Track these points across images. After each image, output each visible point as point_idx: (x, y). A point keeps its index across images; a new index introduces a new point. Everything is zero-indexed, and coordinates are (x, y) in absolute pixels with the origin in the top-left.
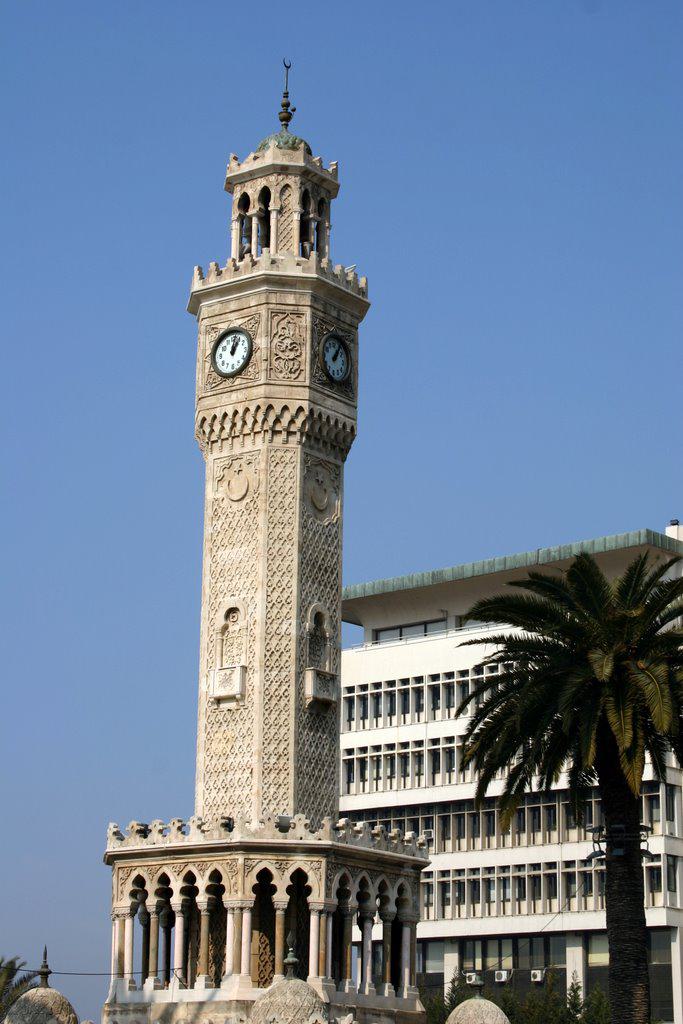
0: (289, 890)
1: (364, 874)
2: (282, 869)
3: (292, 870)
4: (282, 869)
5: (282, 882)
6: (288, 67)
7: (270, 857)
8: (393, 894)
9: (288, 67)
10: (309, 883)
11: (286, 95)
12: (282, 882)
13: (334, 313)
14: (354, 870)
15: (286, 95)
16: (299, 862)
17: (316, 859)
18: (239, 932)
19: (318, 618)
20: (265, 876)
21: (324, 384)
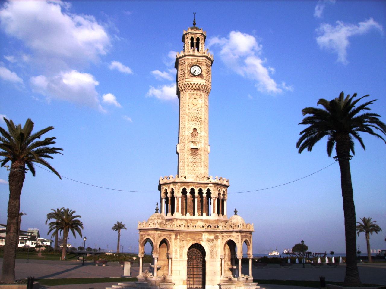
0: (190, 193)
2: (169, 188)
3: (171, 188)
4: (169, 188)
5: (169, 191)
6: (194, 14)
7: (166, 186)
9: (194, 14)
10: (182, 191)
11: (194, 20)
12: (169, 191)
13: (196, 60)
15: (194, 20)
16: (172, 186)
17: (175, 185)
18: (178, 203)
19: (195, 129)
20: (166, 190)
21: (192, 77)
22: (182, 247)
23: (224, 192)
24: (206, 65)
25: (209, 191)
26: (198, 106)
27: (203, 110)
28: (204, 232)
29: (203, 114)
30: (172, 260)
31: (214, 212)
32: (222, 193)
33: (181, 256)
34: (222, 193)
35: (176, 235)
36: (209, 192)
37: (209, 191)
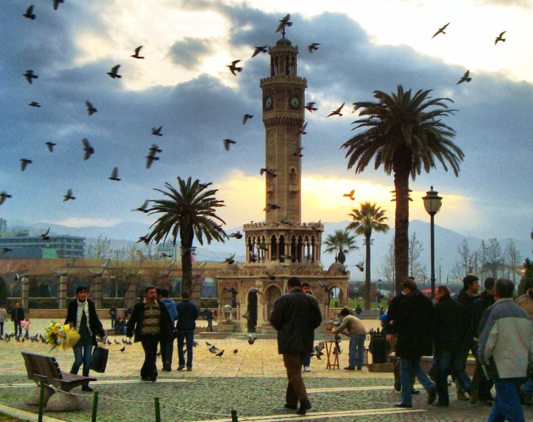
1: (254, 235)
8: (261, 238)
14: (252, 235)
22: (245, 294)
23: (282, 236)
24: (278, 92)
25: (263, 237)
26: (274, 143)
27: (277, 146)
28: (256, 278)
29: (276, 151)
30: (239, 306)
31: (268, 258)
32: (278, 238)
33: (244, 302)
34: (278, 238)
35: (242, 282)
36: (264, 240)
37: (263, 237)
